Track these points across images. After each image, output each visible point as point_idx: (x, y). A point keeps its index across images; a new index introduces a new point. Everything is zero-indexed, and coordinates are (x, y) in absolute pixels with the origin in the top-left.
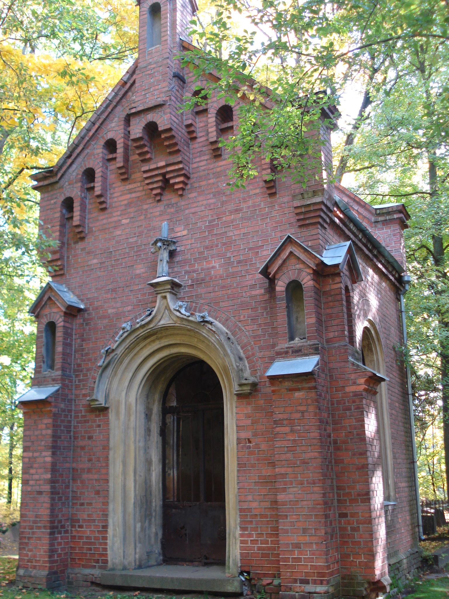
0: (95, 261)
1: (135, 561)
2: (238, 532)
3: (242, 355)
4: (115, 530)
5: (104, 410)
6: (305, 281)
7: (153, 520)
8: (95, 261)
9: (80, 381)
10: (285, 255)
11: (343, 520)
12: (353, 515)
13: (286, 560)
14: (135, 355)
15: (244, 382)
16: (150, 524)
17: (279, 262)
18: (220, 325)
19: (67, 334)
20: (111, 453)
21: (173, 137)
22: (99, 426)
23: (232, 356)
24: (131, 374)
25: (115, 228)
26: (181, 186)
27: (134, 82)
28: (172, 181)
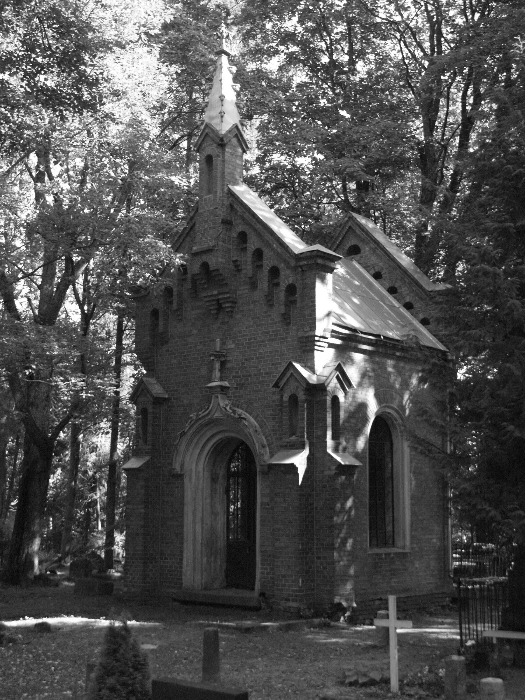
0: (175, 361)
1: (202, 584)
2: (260, 566)
3: (265, 442)
4: (188, 562)
5: (180, 477)
6: (300, 395)
7: (218, 556)
8: (175, 361)
9: (166, 453)
10: (288, 375)
11: (319, 561)
12: (325, 558)
14: (202, 436)
15: (263, 463)
16: (216, 557)
17: (285, 379)
18: (252, 420)
20: (185, 508)
21: (221, 275)
22: (177, 487)
23: (257, 444)
24: (199, 451)
26: (229, 309)
27: (194, 224)
28: (224, 306)
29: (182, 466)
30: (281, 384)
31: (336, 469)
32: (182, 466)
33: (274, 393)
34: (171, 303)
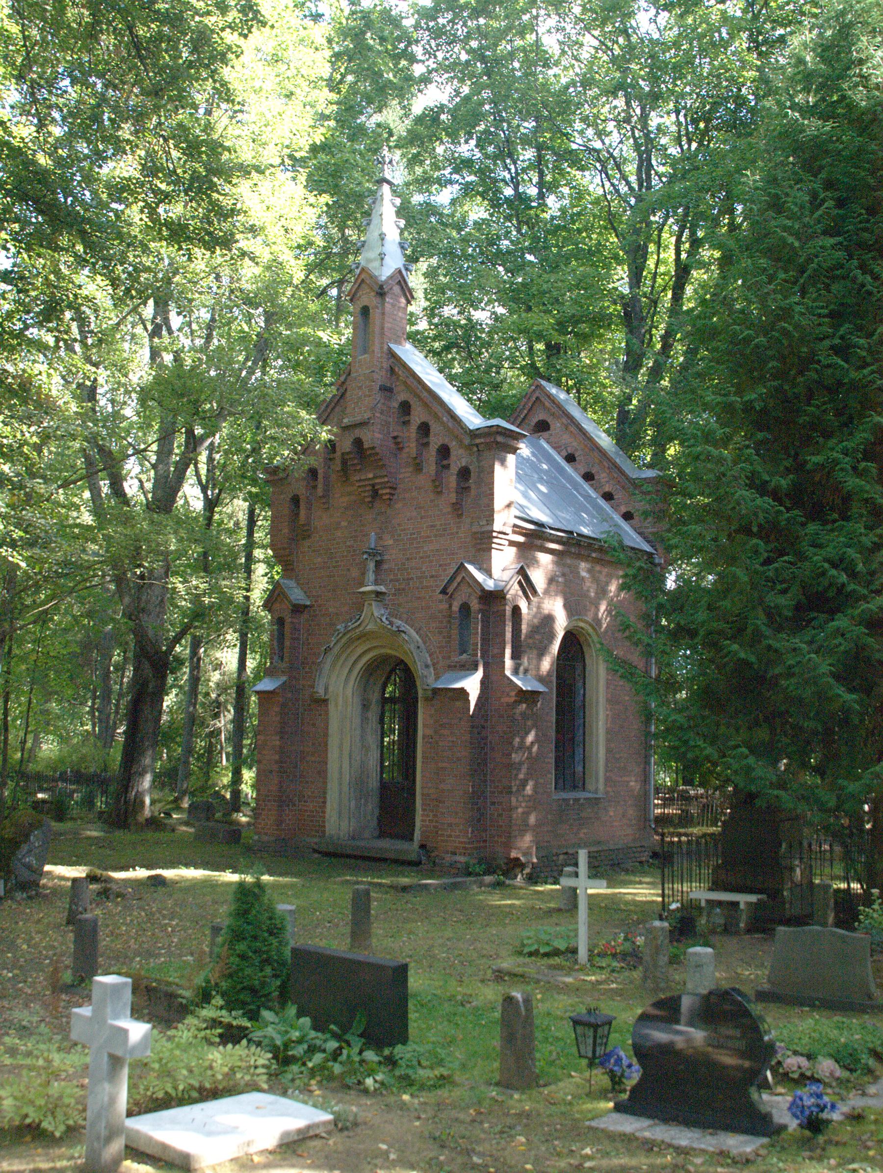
3: (429, 662)
5: (325, 701)
10: (459, 579)
12: (500, 803)
13: (442, 835)
17: (455, 584)
19: (295, 629)
20: (330, 739)
21: (377, 454)
24: (347, 670)
25: (337, 529)
26: (387, 497)
28: (380, 492)
29: (326, 689)
30: (450, 590)
31: (516, 695)
32: (326, 689)
33: (440, 601)
34: (315, 487)
